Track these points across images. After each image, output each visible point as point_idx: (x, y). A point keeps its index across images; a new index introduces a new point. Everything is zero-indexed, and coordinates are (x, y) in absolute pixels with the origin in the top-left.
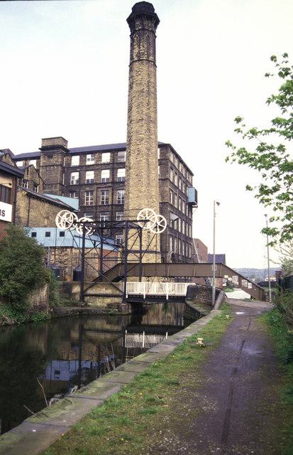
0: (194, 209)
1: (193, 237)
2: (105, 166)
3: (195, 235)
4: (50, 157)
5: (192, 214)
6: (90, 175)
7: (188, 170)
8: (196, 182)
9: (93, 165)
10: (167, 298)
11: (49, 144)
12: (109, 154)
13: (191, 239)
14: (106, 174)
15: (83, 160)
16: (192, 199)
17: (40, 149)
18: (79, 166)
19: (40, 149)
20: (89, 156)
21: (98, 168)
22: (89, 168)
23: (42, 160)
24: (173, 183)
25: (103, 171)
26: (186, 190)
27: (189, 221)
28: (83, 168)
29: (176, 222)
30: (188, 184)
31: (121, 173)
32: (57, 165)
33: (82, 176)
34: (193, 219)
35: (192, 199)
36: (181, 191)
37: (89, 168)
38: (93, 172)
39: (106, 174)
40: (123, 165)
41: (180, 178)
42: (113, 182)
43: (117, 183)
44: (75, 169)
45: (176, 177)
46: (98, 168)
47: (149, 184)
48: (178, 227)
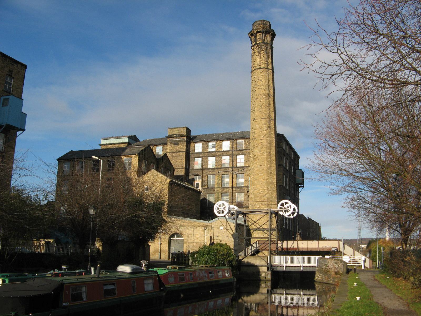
0: (300, 189)
4: (176, 144)
6: (212, 162)
9: (215, 152)
14: (226, 160)
15: (205, 147)
18: (201, 153)
20: (210, 144)
21: (219, 154)
22: (211, 154)
24: (285, 168)
25: (224, 158)
28: (205, 155)
30: (296, 165)
31: (241, 160)
32: (182, 152)
33: (205, 162)
34: (300, 198)
37: (211, 154)
38: (214, 158)
39: (226, 160)
40: (241, 152)
41: (289, 162)
42: (233, 167)
43: (236, 167)
44: (199, 155)
46: (219, 154)
47: (271, 173)
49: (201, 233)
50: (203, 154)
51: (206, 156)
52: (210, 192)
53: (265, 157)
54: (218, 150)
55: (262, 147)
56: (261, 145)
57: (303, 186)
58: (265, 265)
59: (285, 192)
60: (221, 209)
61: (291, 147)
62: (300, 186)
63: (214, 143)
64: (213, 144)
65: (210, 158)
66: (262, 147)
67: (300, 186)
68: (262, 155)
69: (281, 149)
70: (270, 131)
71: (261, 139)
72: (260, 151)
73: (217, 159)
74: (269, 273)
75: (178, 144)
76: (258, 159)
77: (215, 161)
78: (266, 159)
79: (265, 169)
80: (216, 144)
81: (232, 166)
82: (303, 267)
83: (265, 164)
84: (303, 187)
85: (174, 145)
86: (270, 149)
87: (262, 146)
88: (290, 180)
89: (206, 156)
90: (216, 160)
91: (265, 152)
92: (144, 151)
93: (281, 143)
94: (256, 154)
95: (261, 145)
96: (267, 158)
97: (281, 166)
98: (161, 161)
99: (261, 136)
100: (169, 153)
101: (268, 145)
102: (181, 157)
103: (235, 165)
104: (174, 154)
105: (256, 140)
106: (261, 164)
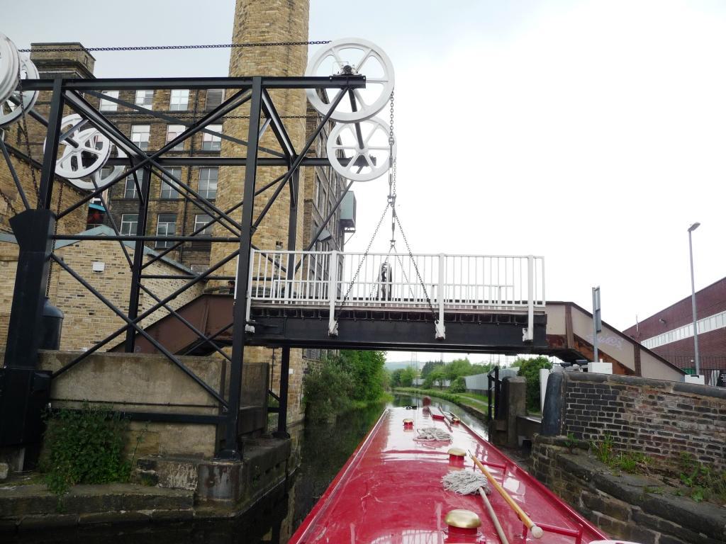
0: (347, 235)
2: (175, 118)
12: (186, 93)
16: (346, 215)
38: (147, 128)
52: (129, 209)
54: (157, 107)
58: (206, 412)
62: (346, 229)
63: (151, 92)
64: (146, 95)
65: (135, 128)
70: (291, 14)
71: (264, 29)
72: (258, 64)
73: (155, 129)
74: (222, 468)
77: (148, 135)
80: (155, 94)
81: (189, 148)
90: (151, 132)
99: (263, 22)
103: (197, 146)
105: (250, 33)
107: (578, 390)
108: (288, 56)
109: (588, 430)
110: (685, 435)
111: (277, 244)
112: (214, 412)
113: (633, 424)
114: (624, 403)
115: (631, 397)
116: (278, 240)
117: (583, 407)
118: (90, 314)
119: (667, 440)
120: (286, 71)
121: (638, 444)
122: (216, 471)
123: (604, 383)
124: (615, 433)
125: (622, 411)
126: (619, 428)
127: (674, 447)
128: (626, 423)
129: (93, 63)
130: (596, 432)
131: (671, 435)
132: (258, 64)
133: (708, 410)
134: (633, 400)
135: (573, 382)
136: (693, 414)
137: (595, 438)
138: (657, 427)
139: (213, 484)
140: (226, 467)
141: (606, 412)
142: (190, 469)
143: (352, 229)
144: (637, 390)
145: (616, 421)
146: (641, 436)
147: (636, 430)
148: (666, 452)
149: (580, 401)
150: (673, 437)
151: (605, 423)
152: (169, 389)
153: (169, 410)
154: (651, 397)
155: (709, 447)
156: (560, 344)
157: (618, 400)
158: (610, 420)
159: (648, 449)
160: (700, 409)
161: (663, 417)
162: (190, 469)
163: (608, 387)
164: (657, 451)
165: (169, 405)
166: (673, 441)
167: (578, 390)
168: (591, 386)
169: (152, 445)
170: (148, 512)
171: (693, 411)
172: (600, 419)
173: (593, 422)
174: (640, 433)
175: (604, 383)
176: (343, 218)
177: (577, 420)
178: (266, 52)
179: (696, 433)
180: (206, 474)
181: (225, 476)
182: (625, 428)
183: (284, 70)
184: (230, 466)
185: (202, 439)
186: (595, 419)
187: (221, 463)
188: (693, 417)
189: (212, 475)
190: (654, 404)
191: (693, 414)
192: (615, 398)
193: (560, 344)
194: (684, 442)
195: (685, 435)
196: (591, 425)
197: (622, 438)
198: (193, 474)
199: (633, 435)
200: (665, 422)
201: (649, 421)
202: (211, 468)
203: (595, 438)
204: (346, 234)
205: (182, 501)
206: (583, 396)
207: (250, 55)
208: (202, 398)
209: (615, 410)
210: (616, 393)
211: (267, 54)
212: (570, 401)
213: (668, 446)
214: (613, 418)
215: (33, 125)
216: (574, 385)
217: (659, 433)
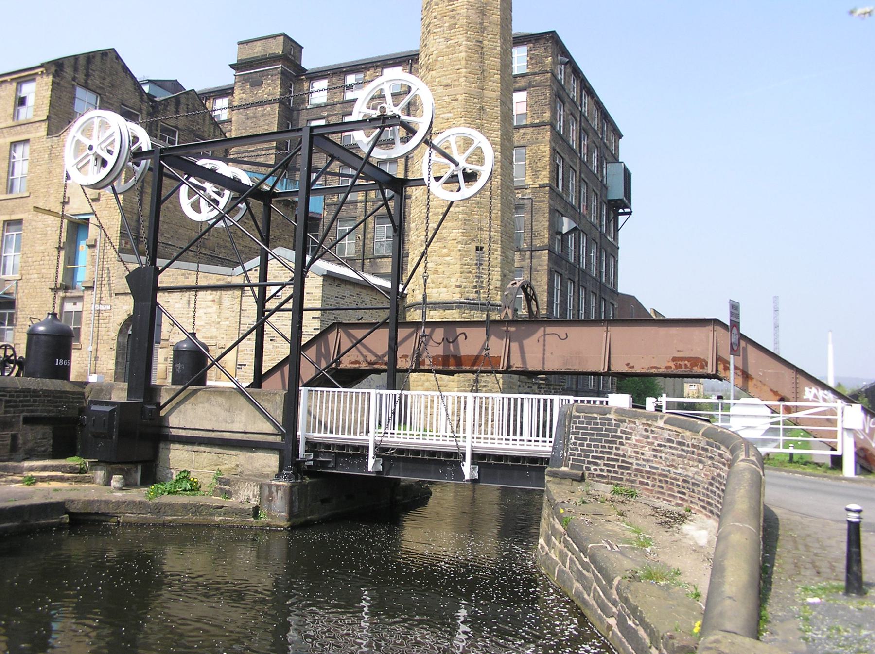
0: (622, 219)
1: (621, 290)
3: (623, 288)
4: (257, 84)
5: (617, 230)
7: (605, 116)
8: (627, 152)
10: (467, 469)
11: (257, 51)
13: (615, 292)
16: (616, 193)
17: (232, 66)
19: (232, 66)
23: (237, 92)
26: (600, 166)
27: (610, 251)
29: (571, 239)
34: (621, 244)
35: (616, 193)
36: (585, 165)
45: (574, 129)
47: (482, 109)
48: (578, 257)
49: (209, 310)
50: (329, 107)
51: (336, 115)
53: (463, 55)
55: (453, 27)
56: (451, 18)
57: (627, 210)
58: (271, 439)
59: (559, 209)
60: (91, 148)
61: (587, 89)
62: (621, 211)
66: (453, 27)
67: (621, 211)
68: (453, 49)
69: (549, 75)
72: (447, 40)
74: (277, 486)
75: (260, 84)
76: (438, 65)
78: (463, 62)
79: (461, 97)
82: (478, 458)
83: (462, 79)
84: (630, 213)
85: (251, 86)
86: (482, 32)
87: (453, 21)
88: (581, 180)
89: (336, 115)
91: (462, 39)
92: (82, 62)
93: (547, 57)
94: (432, 49)
95: (451, 18)
96: (468, 59)
97: (548, 127)
98: (172, 108)
100: (239, 107)
101: (475, 18)
102: (267, 117)
104: (250, 112)
106: (449, 81)
107: (582, 423)
108: (481, 24)
109: (589, 462)
110: (668, 468)
111: (477, 249)
112: (278, 439)
113: (630, 457)
114: (624, 436)
115: (630, 431)
116: (478, 245)
117: (586, 440)
118: (271, 340)
119: (654, 474)
120: (481, 42)
121: (633, 478)
122: (274, 489)
123: (608, 416)
124: (614, 466)
125: (621, 444)
126: (617, 460)
127: (660, 481)
128: (624, 456)
129: (301, 52)
130: (596, 464)
131: (657, 468)
132: (447, 40)
133: (684, 444)
134: (631, 434)
135: (578, 414)
136: (675, 448)
137: (595, 470)
138: (648, 461)
139: (272, 500)
140: (281, 485)
141: (607, 445)
142: (254, 486)
143: (627, 210)
144: (635, 423)
145: (616, 454)
146: (636, 470)
147: (631, 464)
148: (653, 486)
149: (583, 434)
150: (660, 471)
151: (606, 456)
152: (243, 419)
153: (245, 437)
154: (646, 430)
155: (684, 481)
156: (702, 367)
157: (619, 434)
158: (610, 453)
159: (641, 483)
160: (679, 443)
161: (654, 450)
162: (254, 486)
163: (611, 420)
164: (647, 484)
165: (245, 433)
166: (660, 475)
167: (582, 423)
168: (596, 418)
169: (233, 466)
170: (218, 519)
171: (674, 445)
172: (602, 452)
173: (595, 454)
174: (635, 466)
175: (608, 416)
176: (611, 197)
177: (579, 452)
178: (456, 24)
179: (676, 468)
180: (266, 492)
181: (280, 494)
182: (623, 461)
183: (477, 41)
184: (283, 485)
185: (270, 462)
186: (597, 452)
187: (278, 483)
188: (674, 451)
189: (271, 493)
190: (648, 437)
191: (675, 448)
192: (616, 431)
193: (702, 367)
194: (666, 476)
195: (668, 468)
196: (593, 457)
197: (620, 471)
198: (257, 490)
199: (628, 468)
200: (655, 456)
201: (643, 454)
202: (270, 486)
203: (595, 470)
204: (620, 217)
205: (241, 512)
206: (586, 428)
207: (439, 29)
208: (268, 428)
209: (615, 442)
210: (617, 426)
211: (457, 26)
212: (573, 433)
213: (655, 479)
214: (614, 451)
215: (243, 131)
216: (578, 417)
217: (651, 467)
